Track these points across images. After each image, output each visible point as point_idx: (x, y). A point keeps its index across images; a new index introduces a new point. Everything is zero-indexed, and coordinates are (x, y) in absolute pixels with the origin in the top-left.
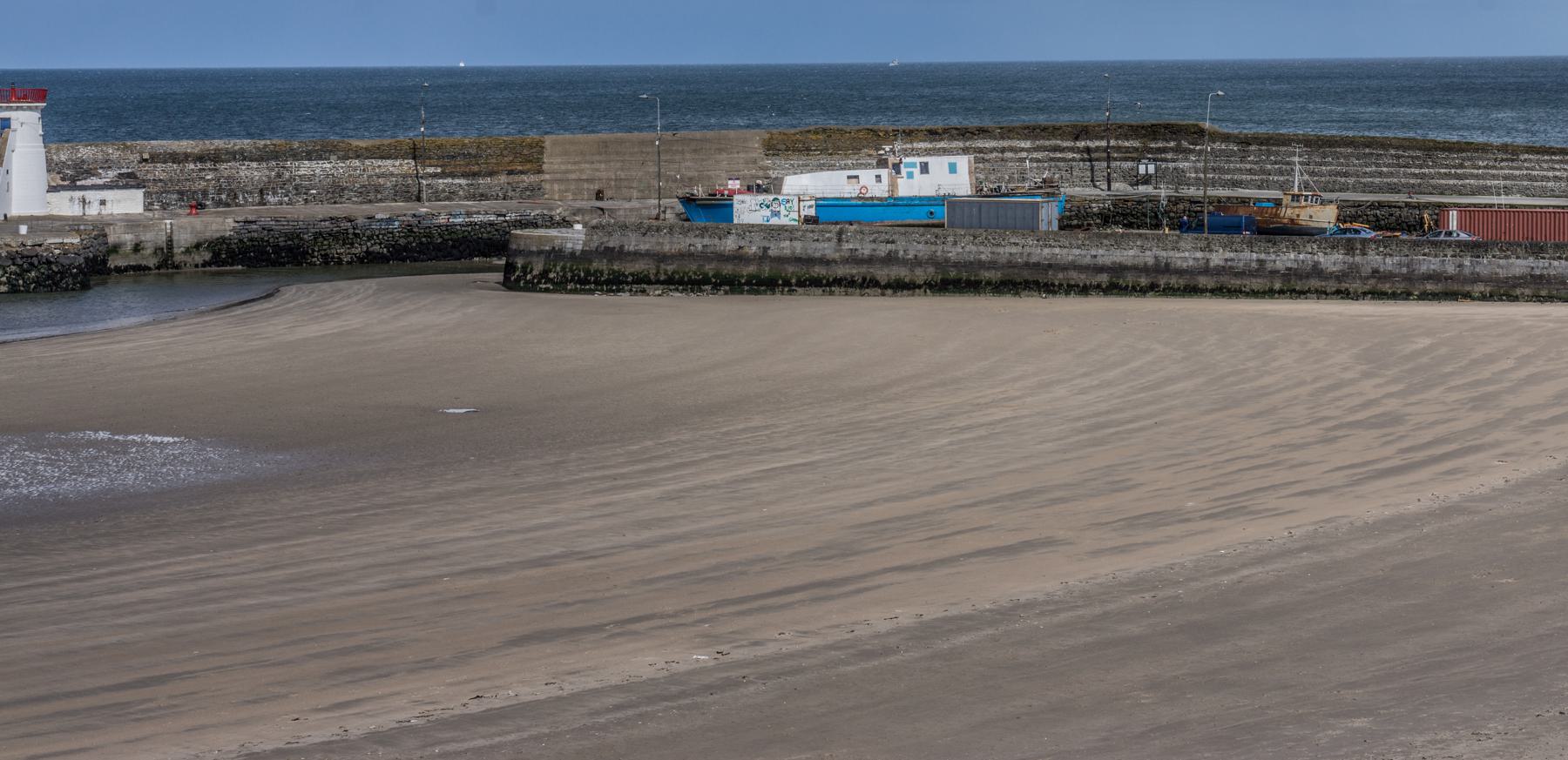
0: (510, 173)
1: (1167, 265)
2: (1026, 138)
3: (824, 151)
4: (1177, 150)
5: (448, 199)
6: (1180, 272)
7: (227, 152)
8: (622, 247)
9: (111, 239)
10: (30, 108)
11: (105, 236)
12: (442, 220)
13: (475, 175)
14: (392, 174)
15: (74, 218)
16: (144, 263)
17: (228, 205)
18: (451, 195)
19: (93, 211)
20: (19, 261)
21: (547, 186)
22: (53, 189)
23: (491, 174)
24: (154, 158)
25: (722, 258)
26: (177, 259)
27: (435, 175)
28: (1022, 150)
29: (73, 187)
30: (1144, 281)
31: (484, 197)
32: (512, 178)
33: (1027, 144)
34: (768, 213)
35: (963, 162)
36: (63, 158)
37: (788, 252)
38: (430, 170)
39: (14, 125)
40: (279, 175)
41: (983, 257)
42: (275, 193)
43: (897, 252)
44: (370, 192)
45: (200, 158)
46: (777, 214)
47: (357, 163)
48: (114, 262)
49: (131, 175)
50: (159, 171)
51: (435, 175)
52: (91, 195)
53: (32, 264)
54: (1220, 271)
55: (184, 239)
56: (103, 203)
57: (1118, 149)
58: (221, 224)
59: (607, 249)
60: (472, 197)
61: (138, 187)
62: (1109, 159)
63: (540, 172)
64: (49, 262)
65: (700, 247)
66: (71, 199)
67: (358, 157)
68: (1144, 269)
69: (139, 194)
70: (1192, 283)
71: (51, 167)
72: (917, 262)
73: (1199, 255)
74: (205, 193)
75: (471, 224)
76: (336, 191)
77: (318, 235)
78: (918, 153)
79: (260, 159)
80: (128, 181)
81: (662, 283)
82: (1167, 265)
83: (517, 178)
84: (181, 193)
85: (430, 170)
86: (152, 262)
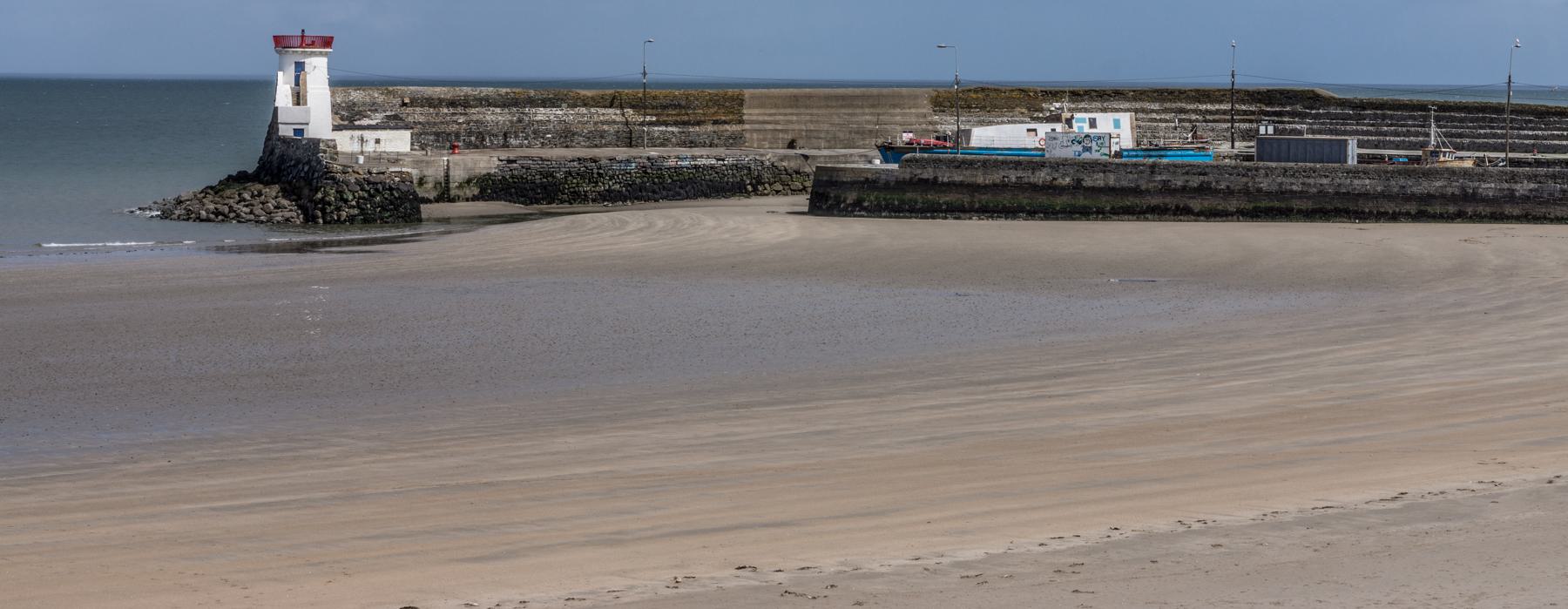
0: (715, 122)
1: (1474, 194)
2: (1154, 100)
3: (983, 108)
4: (1293, 114)
5: (662, 145)
6: (1486, 201)
7: (475, 99)
8: (936, 178)
10: (321, 54)
12: (671, 163)
13: (685, 123)
14: (614, 122)
17: (477, 147)
18: (664, 143)
19: (370, 148)
21: (747, 135)
22: (337, 128)
23: (699, 123)
24: (414, 102)
25: (1034, 187)
26: (453, 192)
27: (651, 124)
28: (1153, 111)
30: (1452, 209)
31: (693, 144)
32: (716, 128)
33: (1156, 106)
34: (1080, 148)
35: (1126, 119)
37: (1101, 183)
38: (648, 118)
40: (520, 121)
41: (1294, 188)
42: (516, 137)
43: (1209, 183)
44: (596, 137)
45: (452, 103)
46: (1089, 149)
47: (584, 110)
49: (396, 117)
50: (417, 115)
51: (651, 124)
52: (367, 134)
53: (377, 190)
54: (1526, 199)
55: (458, 175)
56: (378, 141)
57: (1238, 112)
58: (486, 162)
59: (921, 180)
60: (683, 144)
61: (406, 127)
62: (1233, 121)
63: (741, 122)
64: (391, 189)
65: (1014, 179)
67: (585, 105)
68: (1453, 199)
69: (407, 134)
70: (1499, 210)
71: (336, 109)
72: (1229, 192)
73: (1506, 186)
74: (457, 135)
75: (696, 167)
76: (566, 136)
78: (1086, 110)
79: (503, 106)
80: (394, 122)
81: (977, 211)
82: (1474, 194)
83: (722, 128)
84: (437, 134)
85: (648, 118)
86: (432, 195)
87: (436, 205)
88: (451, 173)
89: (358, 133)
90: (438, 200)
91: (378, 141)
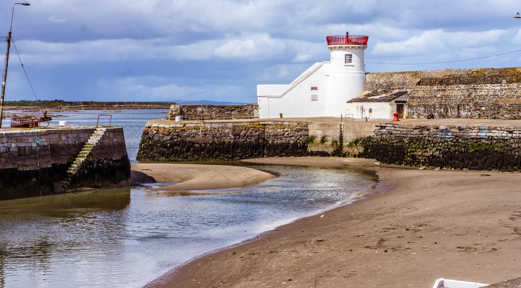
9: (311, 133)
16: (326, 150)
26: (345, 149)
40: (469, 96)
48: (311, 148)
56: (370, 111)
75: (491, 138)
77: (411, 140)
86: (330, 150)
87: (331, 158)
88: (344, 135)
89: (360, 104)
90: (334, 155)
91: (370, 111)
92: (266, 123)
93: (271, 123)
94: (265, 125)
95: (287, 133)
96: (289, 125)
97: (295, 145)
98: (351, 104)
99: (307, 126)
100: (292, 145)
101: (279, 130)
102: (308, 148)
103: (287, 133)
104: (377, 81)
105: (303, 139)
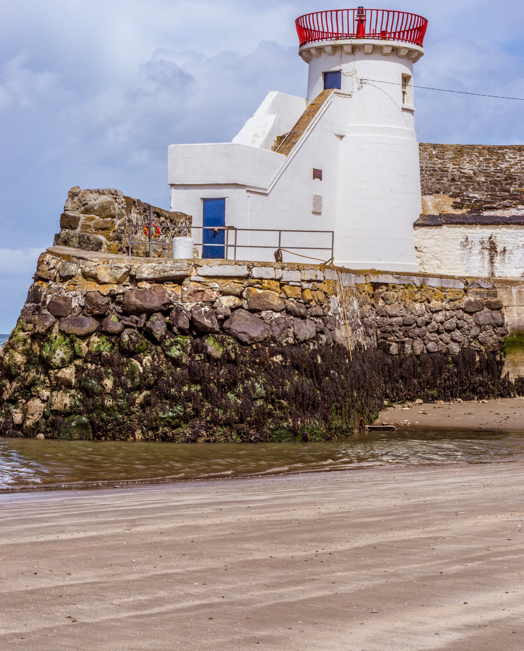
11: (497, 307)
15: (469, 283)
20: (114, 322)
22: (427, 221)
29: (475, 216)
36: (468, 169)
39: (347, 83)
52: (504, 236)
53: (148, 334)
64: (196, 330)
66: (466, 242)
92: (382, 279)
93: (390, 280)
94: (376, 286)
95: (439, 317)
96: (442, 289)
97: (465, 358)
98: (434, 231)
99: (495, 295)
100: (455, 362)
101: (417, 306)
102: (506, 369)
103: (439, 317)
104: (450, 166)
105: (490, 337)
